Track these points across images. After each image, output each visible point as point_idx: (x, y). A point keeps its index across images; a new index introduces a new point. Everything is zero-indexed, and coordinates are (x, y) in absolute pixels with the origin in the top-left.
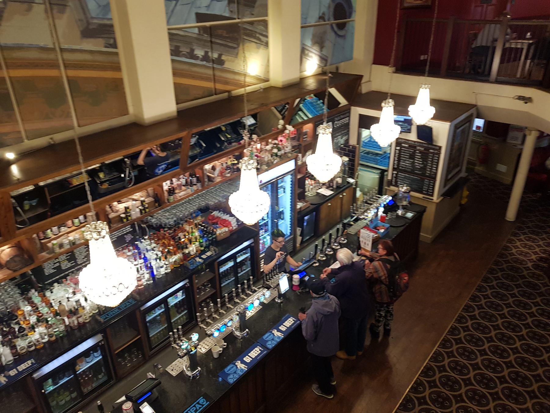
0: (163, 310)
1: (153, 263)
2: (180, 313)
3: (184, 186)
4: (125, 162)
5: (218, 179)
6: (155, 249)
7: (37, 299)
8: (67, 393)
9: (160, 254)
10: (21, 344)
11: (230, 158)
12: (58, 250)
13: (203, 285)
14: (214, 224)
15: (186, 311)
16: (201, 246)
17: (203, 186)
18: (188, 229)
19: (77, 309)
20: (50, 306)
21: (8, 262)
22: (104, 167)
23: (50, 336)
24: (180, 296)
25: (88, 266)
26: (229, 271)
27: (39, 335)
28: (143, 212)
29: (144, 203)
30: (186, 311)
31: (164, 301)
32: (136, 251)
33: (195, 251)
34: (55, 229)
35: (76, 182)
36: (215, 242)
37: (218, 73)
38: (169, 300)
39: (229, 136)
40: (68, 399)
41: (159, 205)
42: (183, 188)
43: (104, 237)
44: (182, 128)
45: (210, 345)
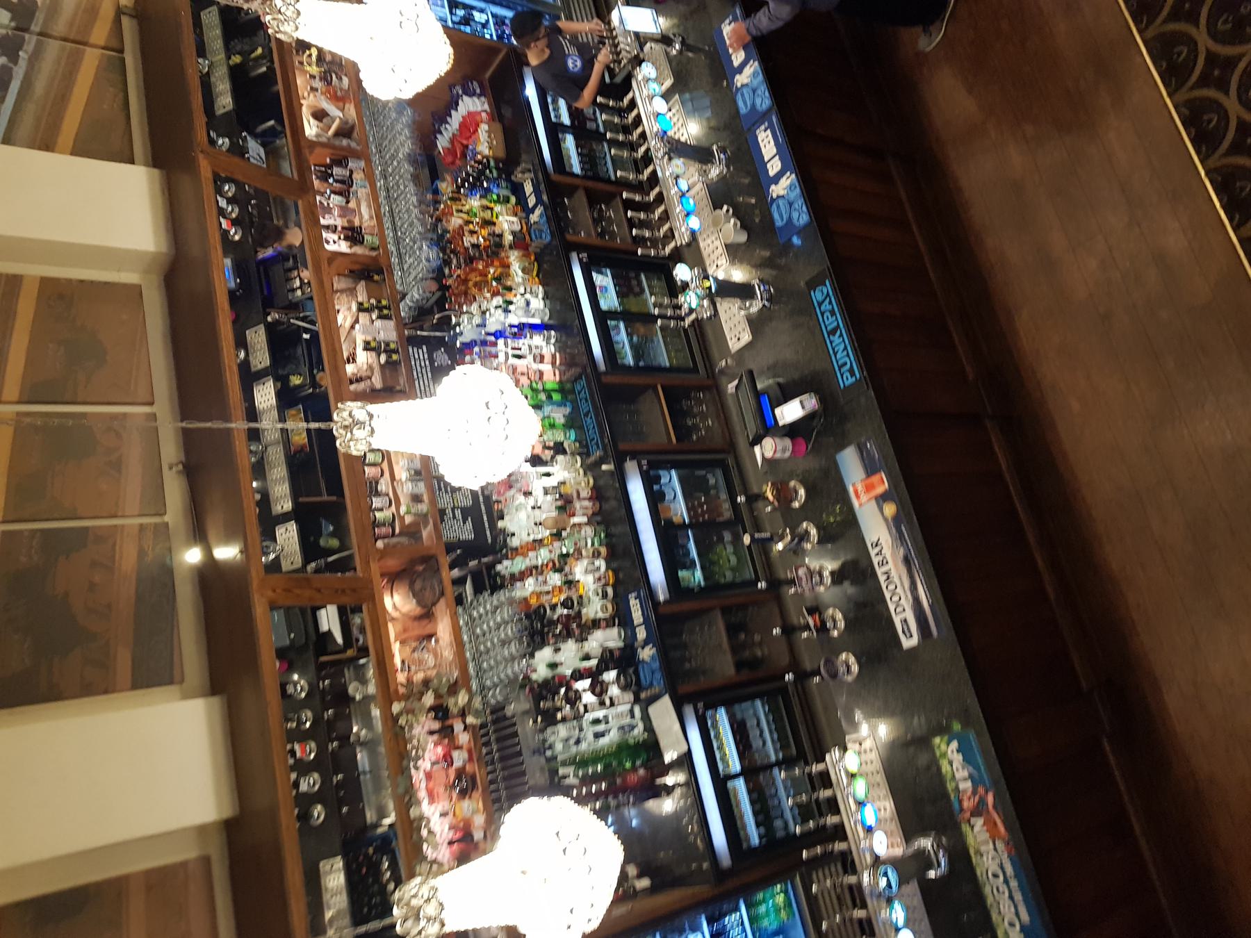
0: (622, 325)
1: (514, 319)
2: (643, 291)
3: (348, 202)
4: (277, 323)
5: (351, 111)
6: (484, 308)
7: (519, 564)
8: (719, 548)
9: (498, 300)
10: (595, 608)
11: (301, 63)
12: (423, 507)
13: (596, 222)
14: (464, 155)
15: (643, 276)
16: (507, 200)
17: (357, 156)
18: (460, 221)
19: (561, 496)
20: (539, 543)
21: (419, 603)
22: (280, 372)
23: (596, 554)
24: (604, 280)
25: (436, 460)
26: (585, 151)
27: (588, 576)
28: (385, 312)
29: (366, 305)
30: (643, 276)
31: (602, 317)
32: (476, 349)
33: (515, 219)
34: (377, 502)
35: (300, 439)
36: (507, 166)
37: (60, 27)
38: (604, 305)
39: (260, 51)
40: (730, 549)
41: (380, 271)
42: (352, 205)
43: (371, 416)
44: (190, 166)
45: (717, 243)
